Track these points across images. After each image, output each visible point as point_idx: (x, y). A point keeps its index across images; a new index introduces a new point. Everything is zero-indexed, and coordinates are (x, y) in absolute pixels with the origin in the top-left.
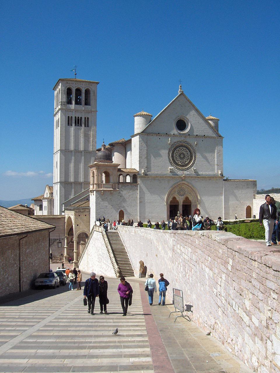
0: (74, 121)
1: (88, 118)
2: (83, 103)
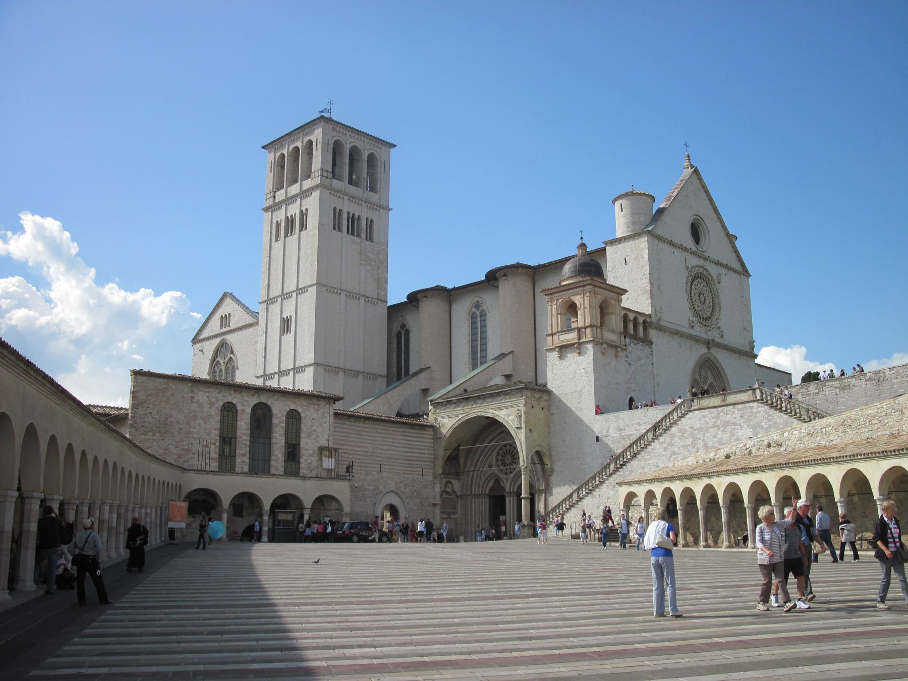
0: (345, 222)
1: (372, 221)
2: (364, 184)
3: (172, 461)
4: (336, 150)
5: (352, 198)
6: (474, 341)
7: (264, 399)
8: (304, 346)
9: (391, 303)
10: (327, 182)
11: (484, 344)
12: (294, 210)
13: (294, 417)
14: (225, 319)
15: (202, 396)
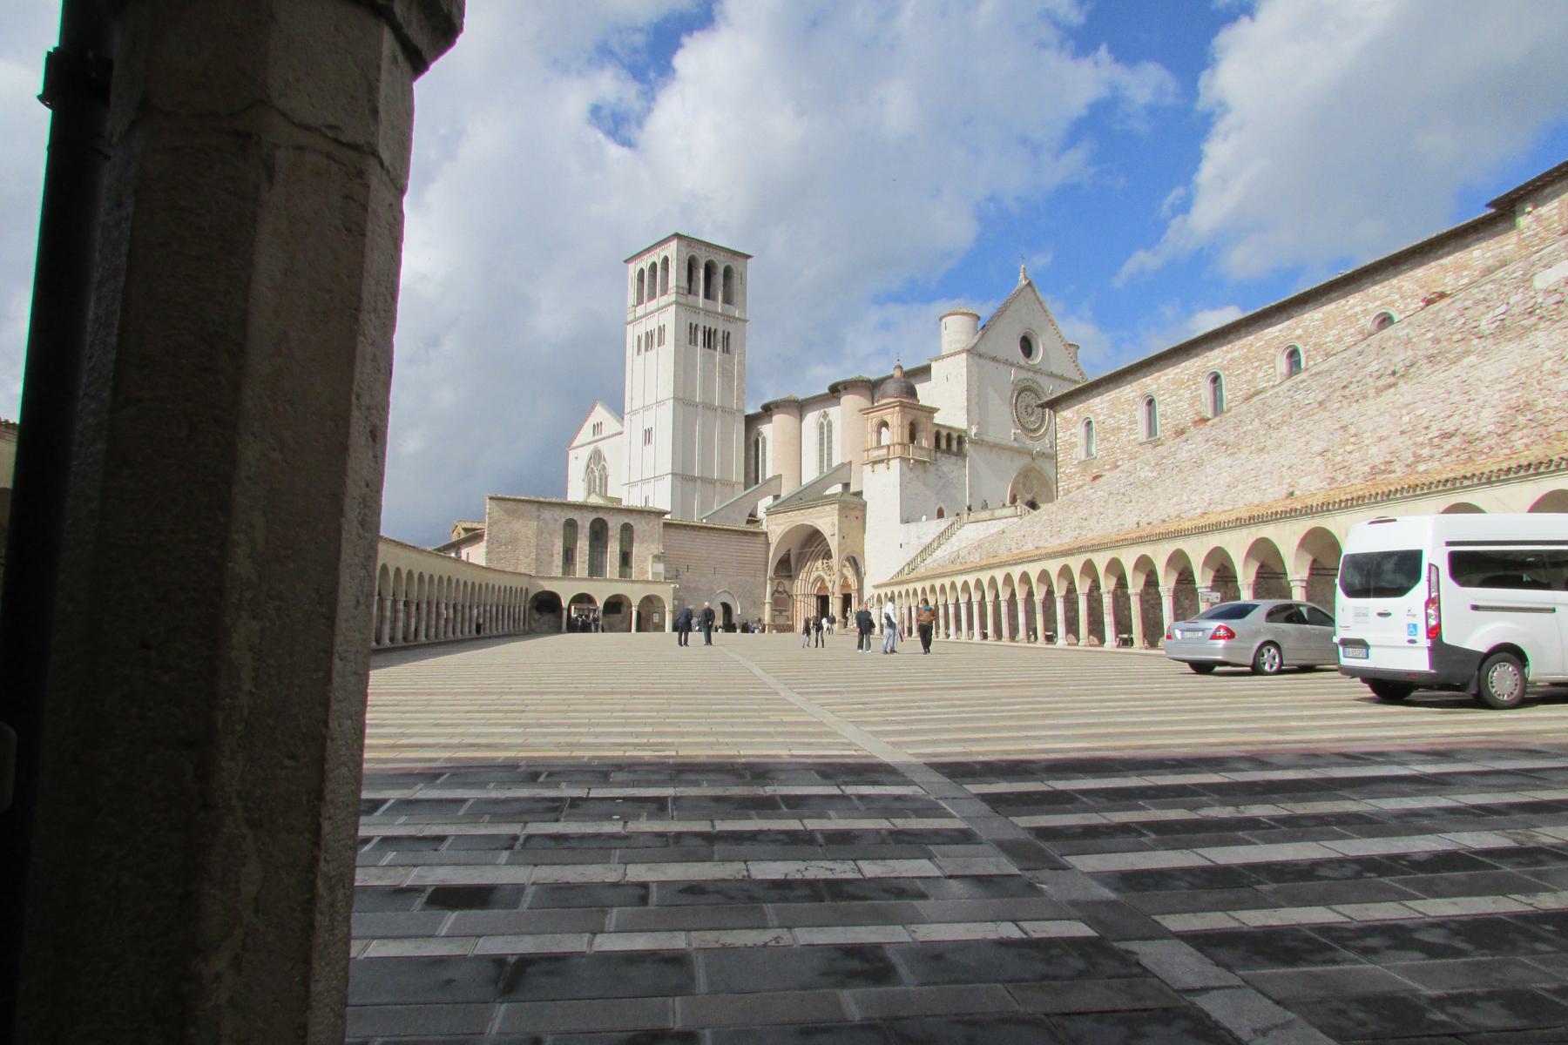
3: (522, 570)
4: (691, 266)
5: (707, 312)
6: (821, 450)
7: (601, 515)
8: (662, 456)
9: (750, 411)
10: (682, 300)
11: (830, 454)
12: (652, 324)
13: (627, 530)
14: (597, 427)
15: (547, 514)
